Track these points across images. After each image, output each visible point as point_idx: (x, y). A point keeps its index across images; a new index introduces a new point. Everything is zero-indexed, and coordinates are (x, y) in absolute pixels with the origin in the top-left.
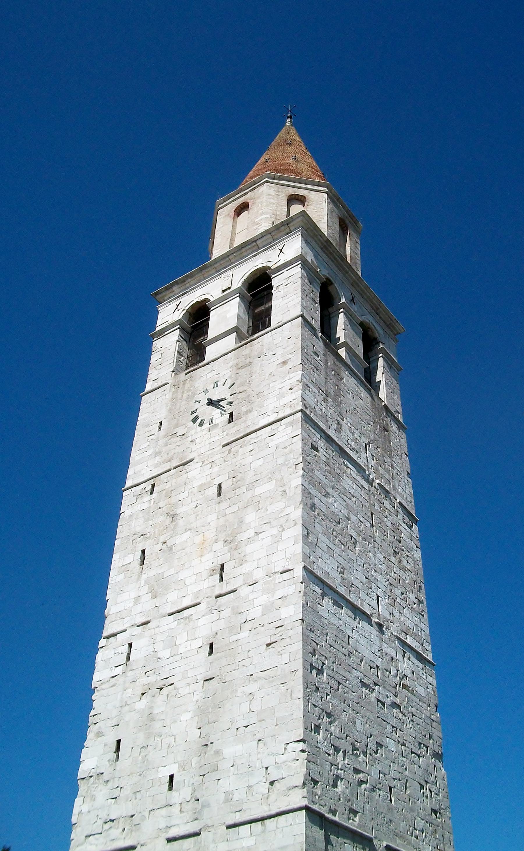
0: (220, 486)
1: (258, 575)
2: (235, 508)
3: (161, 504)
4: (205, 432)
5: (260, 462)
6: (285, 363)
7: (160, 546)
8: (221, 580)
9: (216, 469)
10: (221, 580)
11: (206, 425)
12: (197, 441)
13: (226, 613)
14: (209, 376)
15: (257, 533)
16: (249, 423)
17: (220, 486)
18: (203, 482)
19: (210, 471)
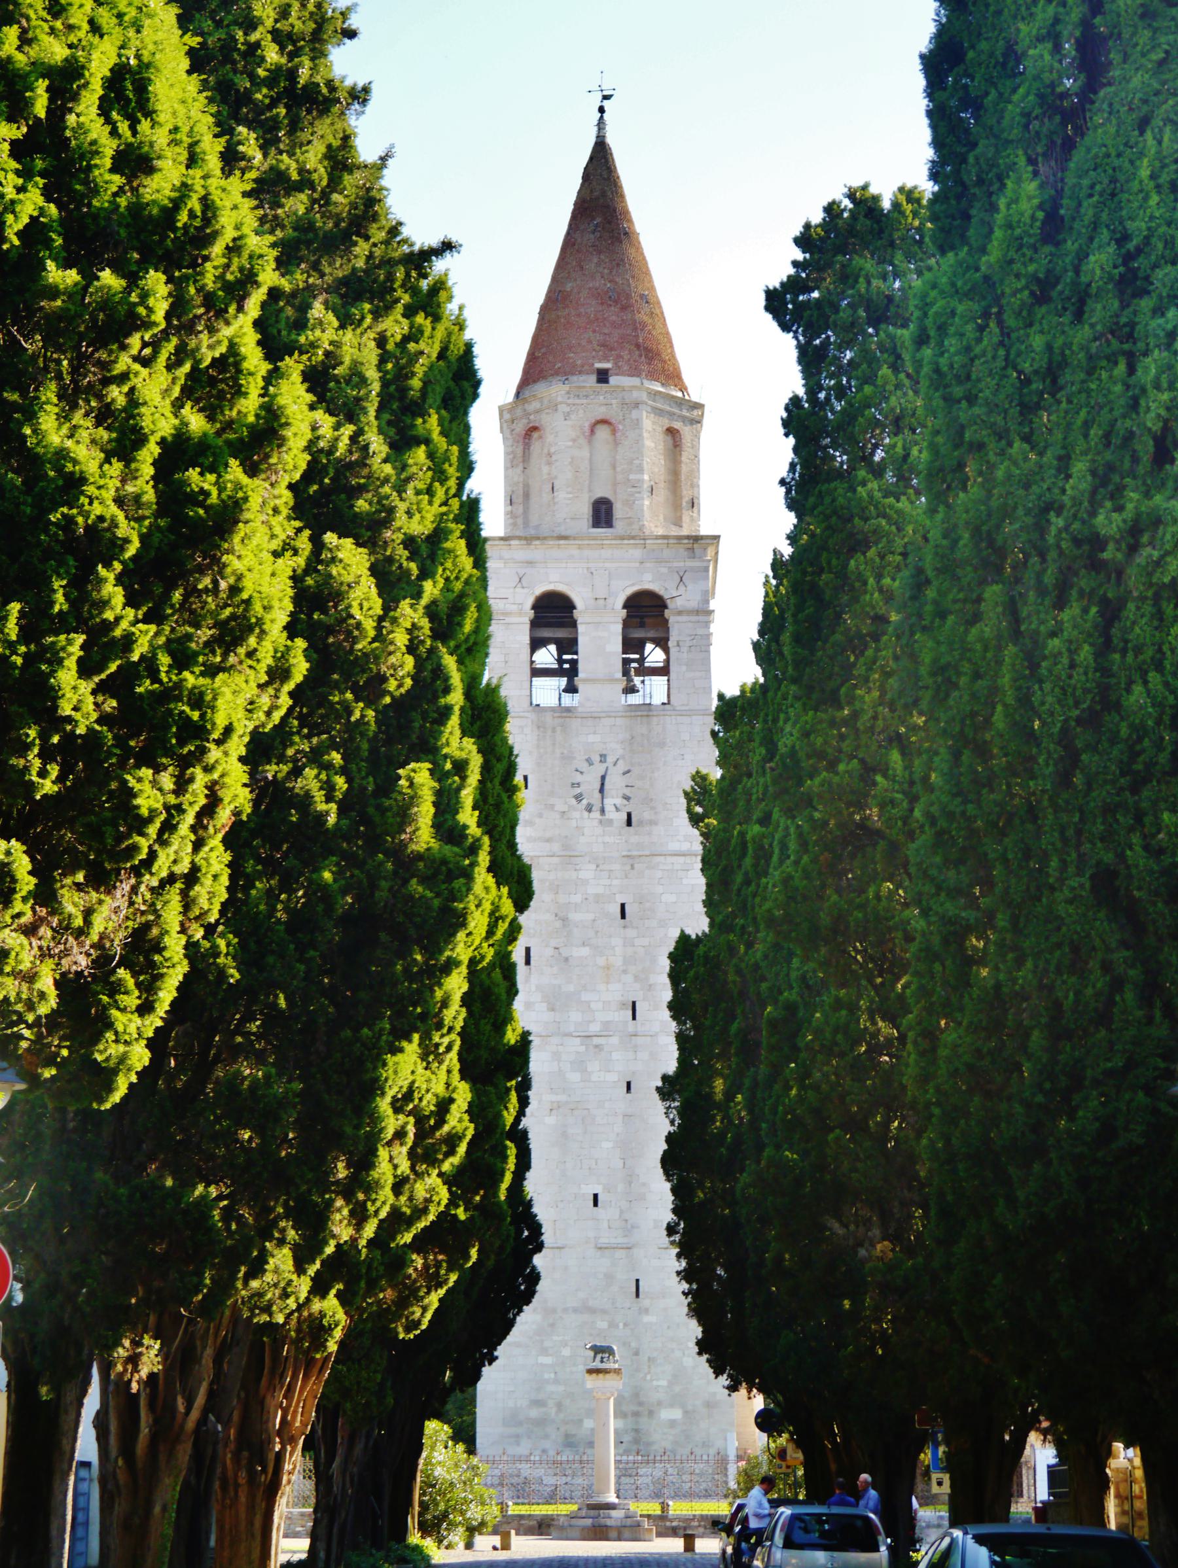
0: (623, 906)
2: (645, 941)
4: (596, 823)
5: (673, 898)
7: (549, 951)
8: (634, 1018)
9: (615, 882)
10: (634, 1018)
12: (586, 831)
14: (591, 738)
17: (623, 906)
18: (600, 890)
19: (607, 882)
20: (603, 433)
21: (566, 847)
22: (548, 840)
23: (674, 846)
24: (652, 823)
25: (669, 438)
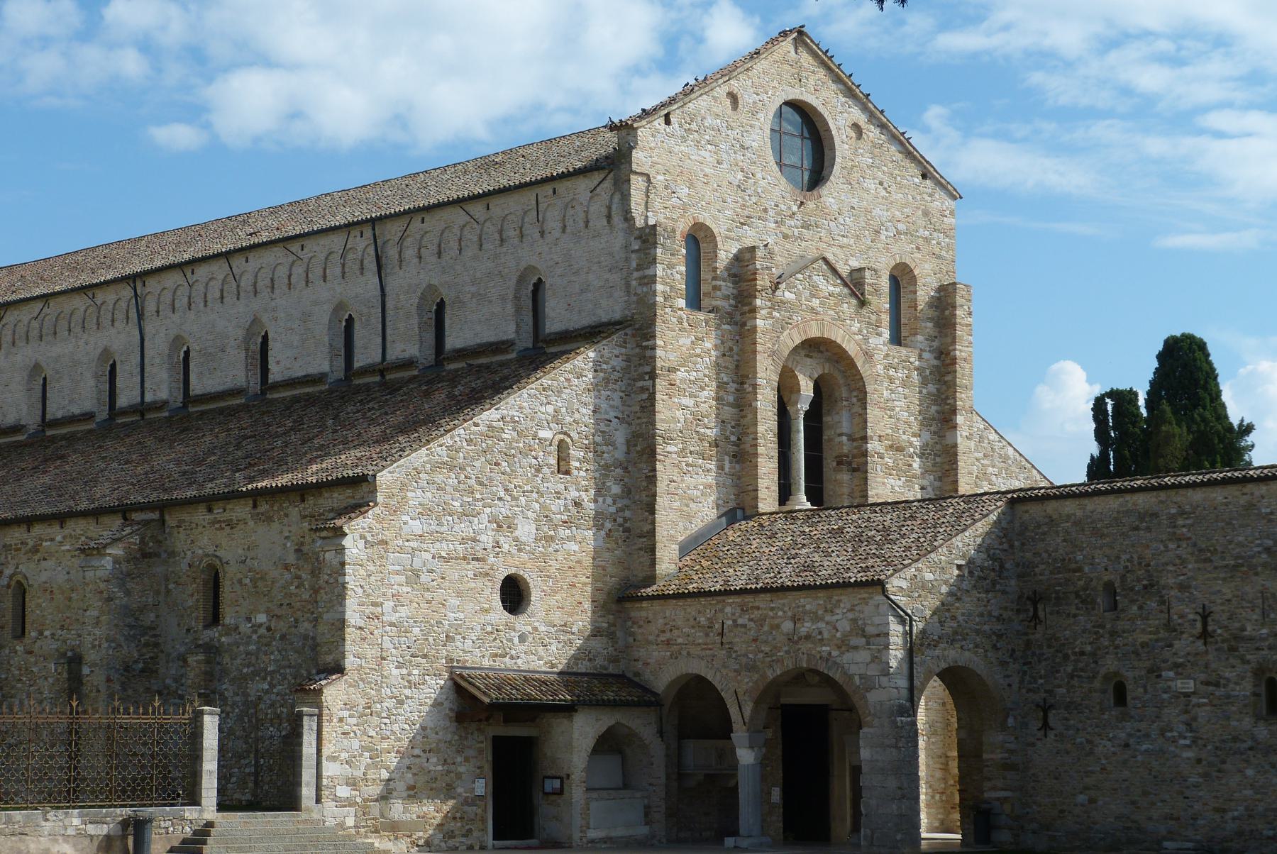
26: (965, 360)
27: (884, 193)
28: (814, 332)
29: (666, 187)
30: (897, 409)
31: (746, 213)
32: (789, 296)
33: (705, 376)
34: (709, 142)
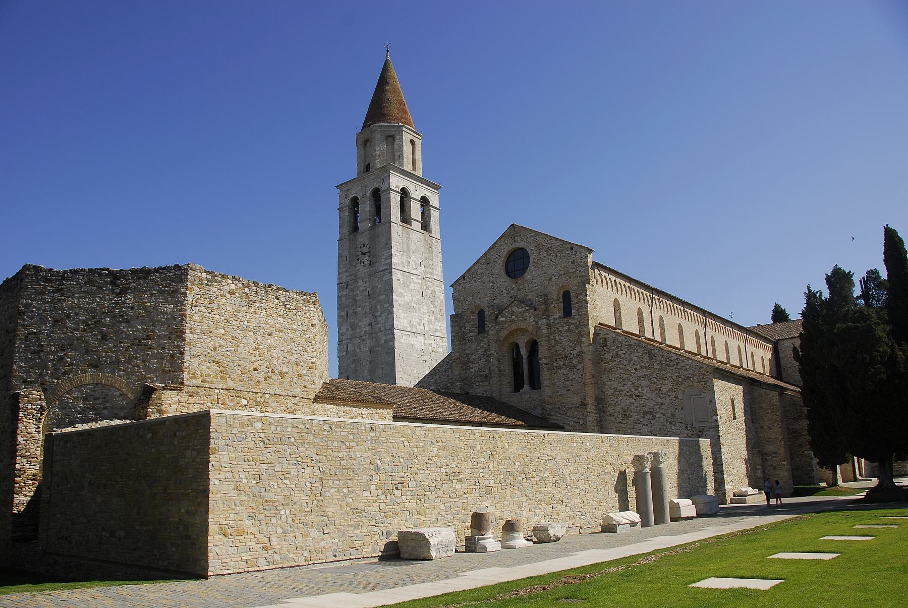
1: (382, 329)
2: (374, 302)
3: (351, 294)
4: (362, 267)
6: (387, 244)
11: (362, 264)
13: (374, 340)
15: (381, 314)
16: (376, 268)
19: (365, 285)
20: (368, 144)
21: (355, 277)
22: (351, 275)
23: (381, 269)
24: (376, 262)
25: (390, 139)
26: (585, 314)
27: (552, 263)
28: (514, 327)
29: (464, 300)
30: (564, 343)
31: (494, 295)
32: (502, 319)
33: (482, 355)
34: (479, 279)
